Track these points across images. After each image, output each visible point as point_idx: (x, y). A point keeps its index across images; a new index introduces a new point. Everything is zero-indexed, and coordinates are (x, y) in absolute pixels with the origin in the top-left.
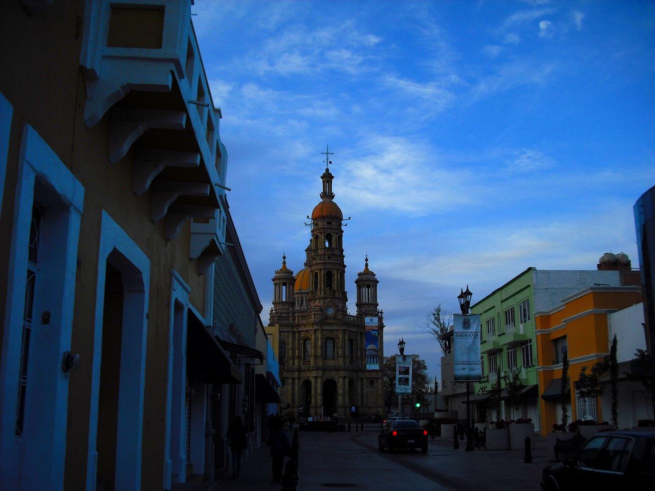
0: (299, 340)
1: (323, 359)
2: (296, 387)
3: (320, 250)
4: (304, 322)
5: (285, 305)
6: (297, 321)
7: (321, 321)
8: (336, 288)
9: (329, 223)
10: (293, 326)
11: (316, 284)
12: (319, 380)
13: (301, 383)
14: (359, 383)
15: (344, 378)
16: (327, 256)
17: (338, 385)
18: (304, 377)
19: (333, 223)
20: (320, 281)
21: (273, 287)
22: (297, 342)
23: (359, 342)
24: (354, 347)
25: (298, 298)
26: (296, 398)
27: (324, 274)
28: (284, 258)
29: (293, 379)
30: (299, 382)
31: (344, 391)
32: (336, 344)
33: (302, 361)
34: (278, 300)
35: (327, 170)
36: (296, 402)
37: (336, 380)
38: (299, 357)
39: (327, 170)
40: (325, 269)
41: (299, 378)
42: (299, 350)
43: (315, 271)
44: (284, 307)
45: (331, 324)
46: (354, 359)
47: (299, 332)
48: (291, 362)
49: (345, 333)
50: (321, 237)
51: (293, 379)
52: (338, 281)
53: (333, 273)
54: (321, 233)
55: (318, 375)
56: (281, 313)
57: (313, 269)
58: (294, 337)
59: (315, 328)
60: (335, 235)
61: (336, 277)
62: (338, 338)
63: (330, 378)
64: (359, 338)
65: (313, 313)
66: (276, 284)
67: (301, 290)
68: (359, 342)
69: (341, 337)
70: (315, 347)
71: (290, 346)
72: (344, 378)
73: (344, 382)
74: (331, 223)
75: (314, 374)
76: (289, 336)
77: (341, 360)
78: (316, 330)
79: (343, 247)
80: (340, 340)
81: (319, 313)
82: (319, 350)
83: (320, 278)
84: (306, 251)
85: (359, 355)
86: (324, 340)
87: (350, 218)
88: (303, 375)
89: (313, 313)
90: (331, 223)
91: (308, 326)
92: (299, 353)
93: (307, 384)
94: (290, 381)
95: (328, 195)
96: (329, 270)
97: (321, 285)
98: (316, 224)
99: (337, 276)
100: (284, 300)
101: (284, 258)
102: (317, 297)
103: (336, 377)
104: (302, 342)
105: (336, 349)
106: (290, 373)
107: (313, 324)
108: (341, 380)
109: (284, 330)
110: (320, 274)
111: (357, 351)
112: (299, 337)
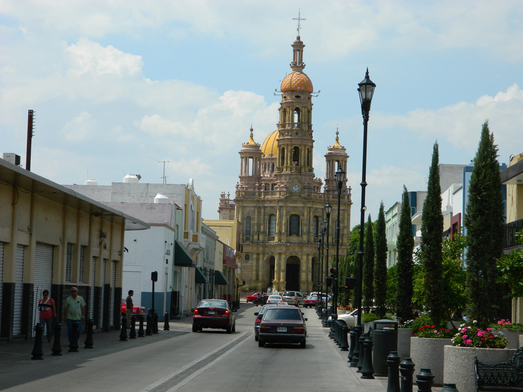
1: (287, 236)
2: (261, 262)
3: (287, 125)
4: (269, 197)
6: (262, 197)
7: (286, 198)
8: (302, 164)
9: (298, 97)
10: (259, 201)
11: (283, 158)
12: (283, 256)
13: (265, 258)
16: (295, 132)
19: (302, 96)
20: (287, 157)
21: (240, 159)
22: (262, 217)
25: (269, 164)
26: (260, 273)
27: (291, 150)
28: (252, 130)
31: (308, 268)
33: (267, 237)
34: (243, 175)
35: (299, 38)
36: (260, 278)
37: (300, 257)
38: (264, 232)
39: (299, 38)
40: (292, 145)
41: (264, 254)
43: (282, 146)
45: (296, 202)
47: (265, 207)
48: (256, 237)
49: (310, 211)
50: (289, 112)
51: (258, 254)
52: (305, 158)
53: (300, 148)
54: (289, 107)
55: (281, 251)
56: (247, 188)
58: (259, 213)
59: (280, 205)
61: (303, 154)
62: (303, 216)
63: (294, 254)
65: (278, 190)
66: (242, 158)
67: (272, 155)
69: (305, 214)
70: (280, 224)
71: (256, 222)
72: (308, 255)
73: (307, 259)
74: (300, 97)
75: (278, 250)
79: (313, 123)
80: (305, 217)
81: (284, 189)
82: (283, 227)
83: (287, 154)
84: (285, 91)
88: (267, 250)
89: (278, 190)
90: (300, 97)
92: (264, 229)
93: (272, 259)
94: (255, 256)
95: (298, 65)
97: (288, 160)
98: (285, 97)
99: (305, 152)
100: (250, 174)
101: (252, 130)
102: (283, 173)
103: (300, 254)
104: (267, 217)
108: (305, 257)
110: (287, 149)
112: (264, 213)
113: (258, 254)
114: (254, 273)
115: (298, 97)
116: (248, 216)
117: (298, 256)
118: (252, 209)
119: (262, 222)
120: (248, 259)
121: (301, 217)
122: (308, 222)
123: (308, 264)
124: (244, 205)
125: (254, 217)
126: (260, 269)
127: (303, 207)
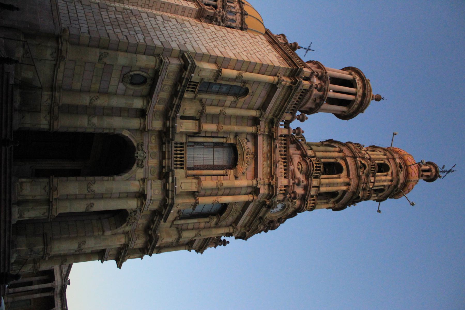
0: (236, 135)
3: (372, 179)
13: (126, 134)
18: (142, 144)
29: (142, 113)
30: (129, 130)
32: (208, 220)
37: (120, 230)
44: (313, 97)
45: (255, 214)
47: (255, 136)
51: (142, 113)
53: (332, 200)
54: (391, 181)
57: (349, 160)
59: (262, 191)
71: (230, 111)
76: (253, 109)
78: (255, 191)
87: (379, 211)
91: (265, 163)
94: (138, 103)
96: (339, 196)
106: (161, 107)
107: (270, 185)
109: (273, 100)
114: (85, 100)
117: (125, 225)
120: (132, 83)
124: (279, 90)
125: (239, 105)
126: (95, 120)
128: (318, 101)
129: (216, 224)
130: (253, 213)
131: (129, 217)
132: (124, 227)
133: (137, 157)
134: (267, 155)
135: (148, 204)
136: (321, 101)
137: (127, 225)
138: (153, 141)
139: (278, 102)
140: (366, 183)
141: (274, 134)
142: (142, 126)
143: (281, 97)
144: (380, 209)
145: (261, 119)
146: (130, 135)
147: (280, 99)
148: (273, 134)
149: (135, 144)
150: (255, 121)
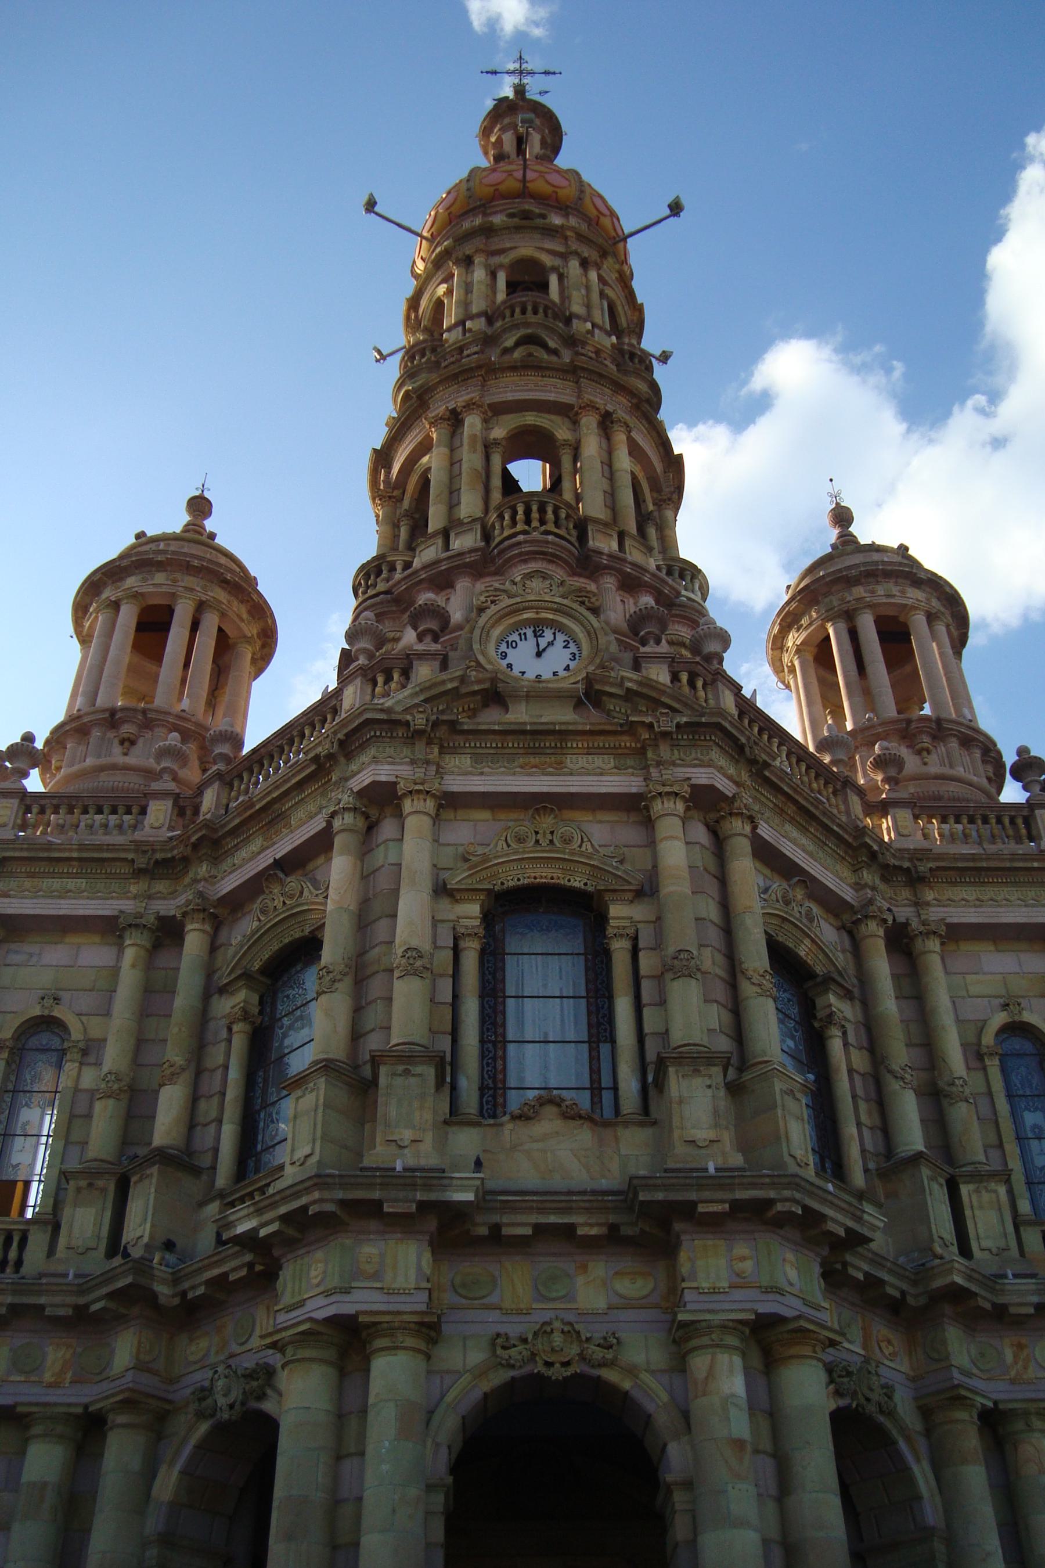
1: (454, 1117)
5: (128, 742)
14: (975, 1478)
15: (767, 1339)
17: (676, 1456)
18: (204, 1393)
23: (889, 1003)
24: (836, 1046)
30: (150, 1472)
32: (619, 948)
37: (654, 1394)
38: (183, 1161)
41: (156, 1416)
42: (194, 1099)
45: (541, 743)
46: (858, 1178)
53: (562, 433)
54: (467, 262)
60: (574, 264)
62: (647, 890)
64: (882, 966)
68: (889, 1003)
77: (697, 1106)
85: (913, 1136)
86: (474, 909)
87: (676, 208)
90: (543, 216)
92: (192, 1123)
96: (530, 418)
105: (623, 1007)
106: (55, 1354)
111: (881, 1103)
113: (88, 1429)
115: (526, 215)
116: (48, 1023)
118: (94, 954)
119: (175, 1054)
121: (618, 912)
122: (711, 960)
123: (784, 1484)
127: (635, 807)
128: (127, 729)
129: (639, 894)
130: (535, 751)
131: (540, 1368)
132: (631, 1371)
133: (231, 1406)
134: (271, 823)
135: (376, 1296)
136: (123, 721)
137: (603, 1364)
138: (204, 1343)
139: (71, 884)
140: (461, 349)
141: (194, 839)
142: (121, 1419)
143: (46, 883)
144: (668, 212)
145: (150, 920)
146: (172, 1463)
147: (56, 884)
148: (195, 846)
149: (204, 1428)
150: (167, 933)
